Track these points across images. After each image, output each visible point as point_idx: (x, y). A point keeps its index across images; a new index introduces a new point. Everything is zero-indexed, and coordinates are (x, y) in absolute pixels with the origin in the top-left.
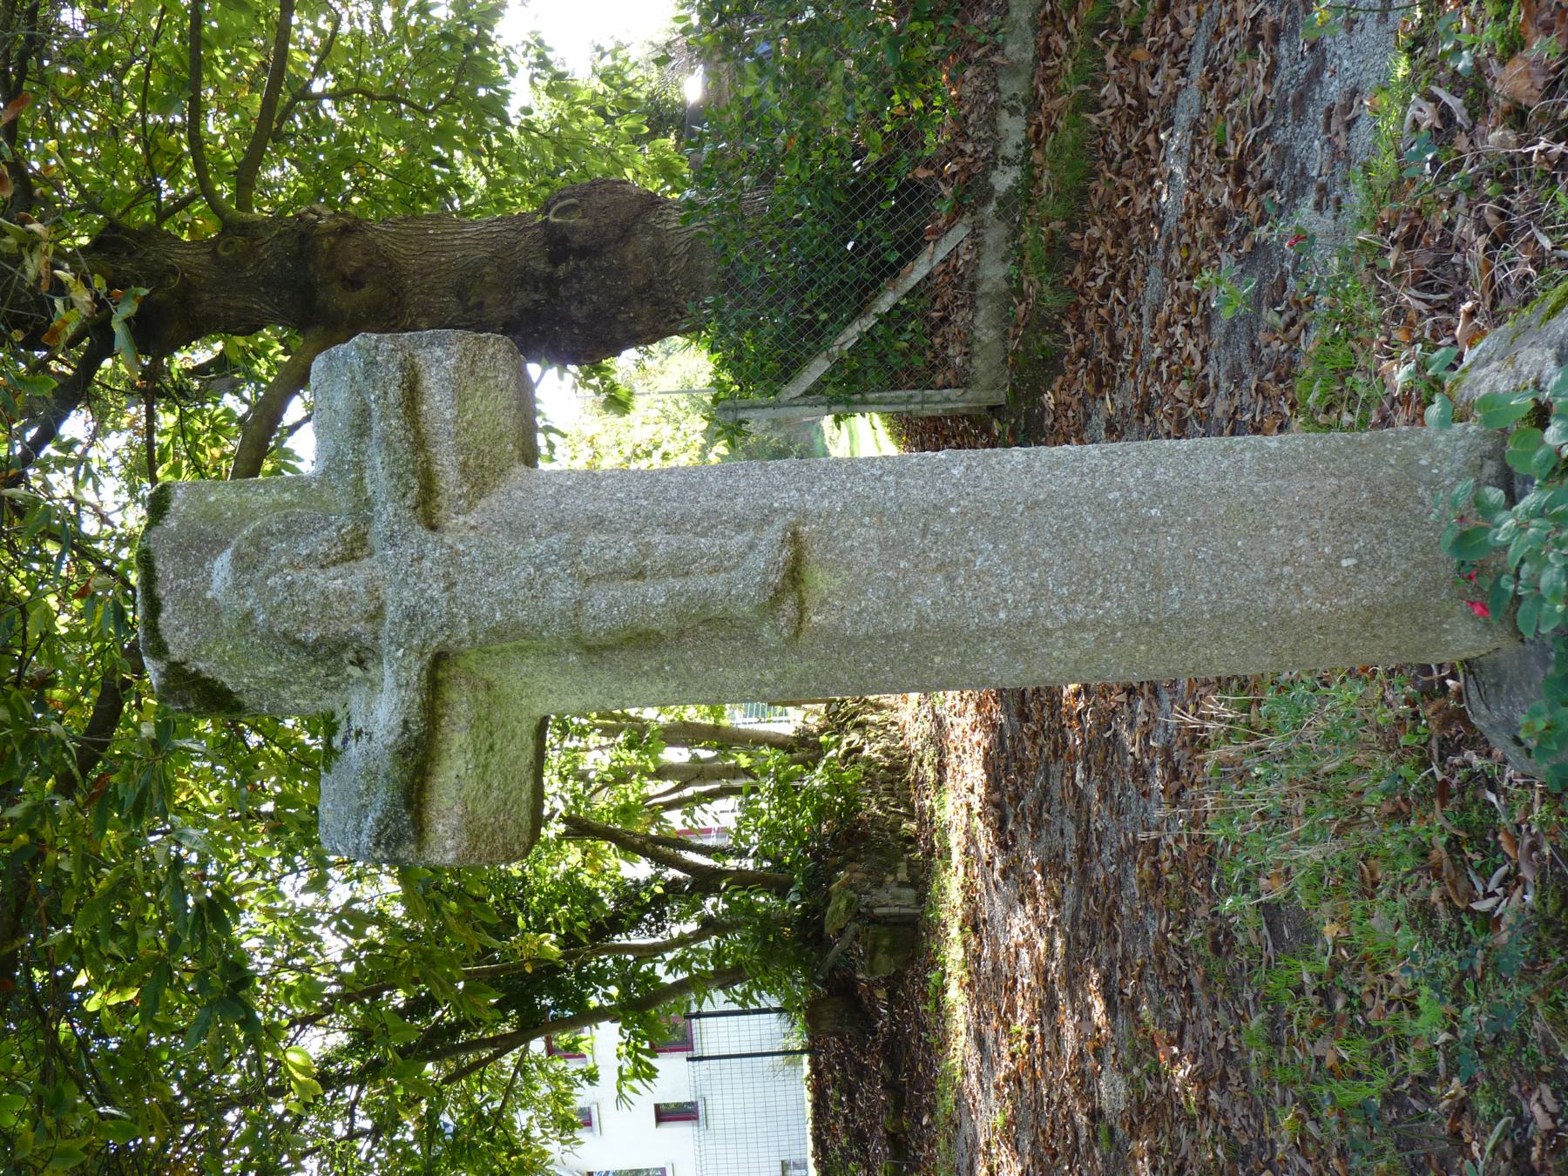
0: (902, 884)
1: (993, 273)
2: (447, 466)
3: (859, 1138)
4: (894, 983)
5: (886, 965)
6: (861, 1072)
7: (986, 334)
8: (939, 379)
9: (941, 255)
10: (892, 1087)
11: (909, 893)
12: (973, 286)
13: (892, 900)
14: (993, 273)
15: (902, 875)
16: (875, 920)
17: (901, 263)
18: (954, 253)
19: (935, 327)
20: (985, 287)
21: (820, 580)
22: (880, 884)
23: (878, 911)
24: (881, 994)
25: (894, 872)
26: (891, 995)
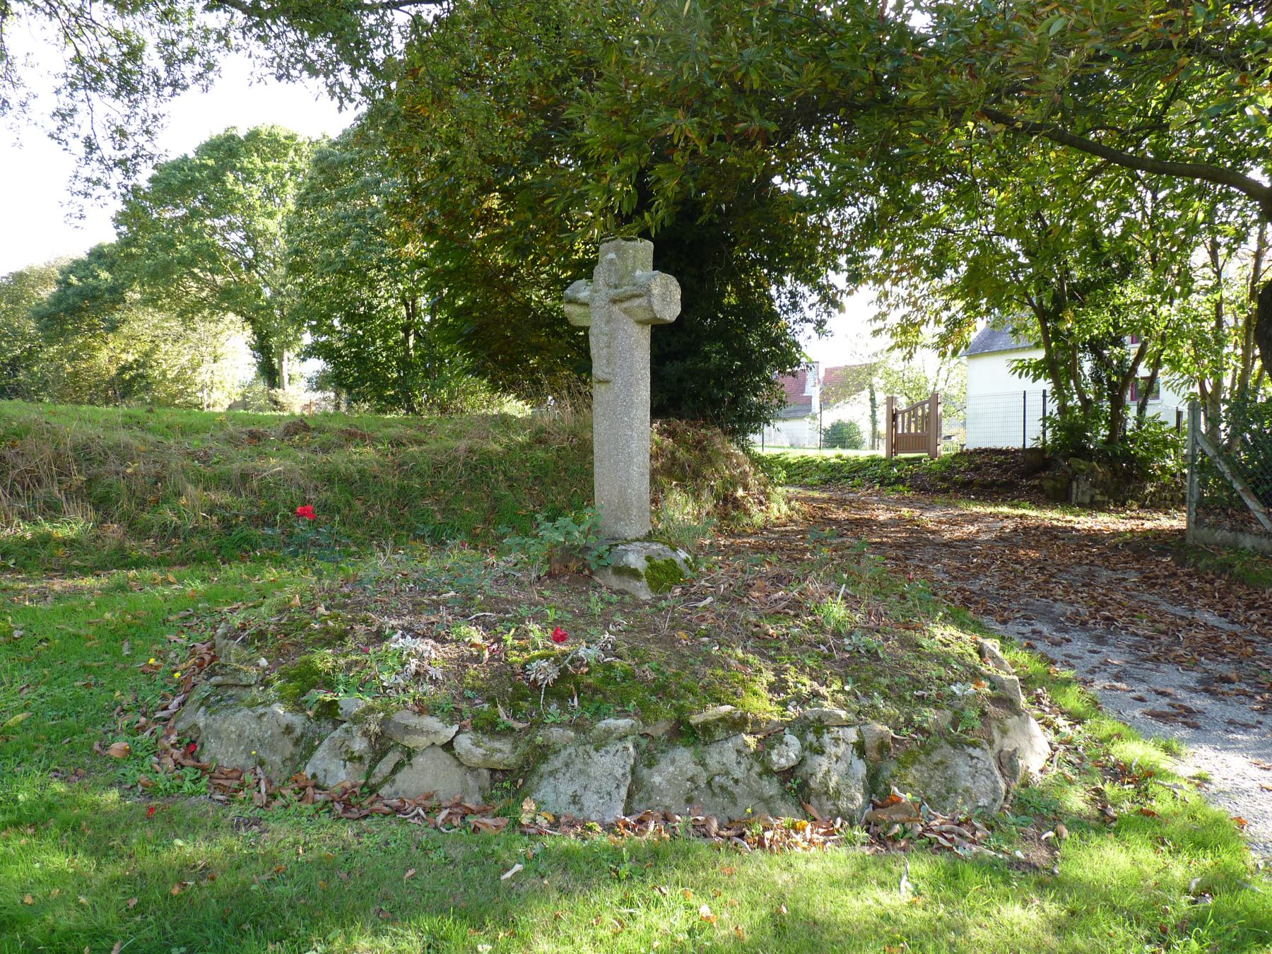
0: (1092, 497)
1: (1248, 542)
2: (626, 305)
3: (977, 468)
4: (1040, 488)
5: (1048, 484)
6: (1006, 471)
7: (1219, 535)
8: (1200, 511)
9: (1258, 515)
10: (993, 483)
11: (1087, 500)
12: (1241, 530)
13: (1080, 489)
14: (1248, 542)
15: (1099, 498)
16: (1070, 482)
17: (1256, 494)
18: (1258, 522)
19: (1224, 510)
20: (1241, 537)
21: (603, 387)
22: (1094, 486)
23: (1075, 484)
24: (1037, 482)
25: (1102, 494)
26: (1035, 487)
